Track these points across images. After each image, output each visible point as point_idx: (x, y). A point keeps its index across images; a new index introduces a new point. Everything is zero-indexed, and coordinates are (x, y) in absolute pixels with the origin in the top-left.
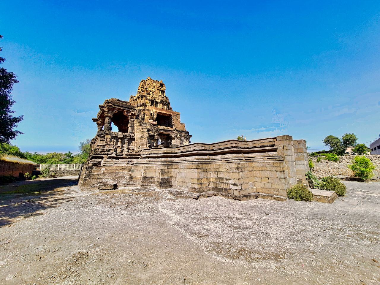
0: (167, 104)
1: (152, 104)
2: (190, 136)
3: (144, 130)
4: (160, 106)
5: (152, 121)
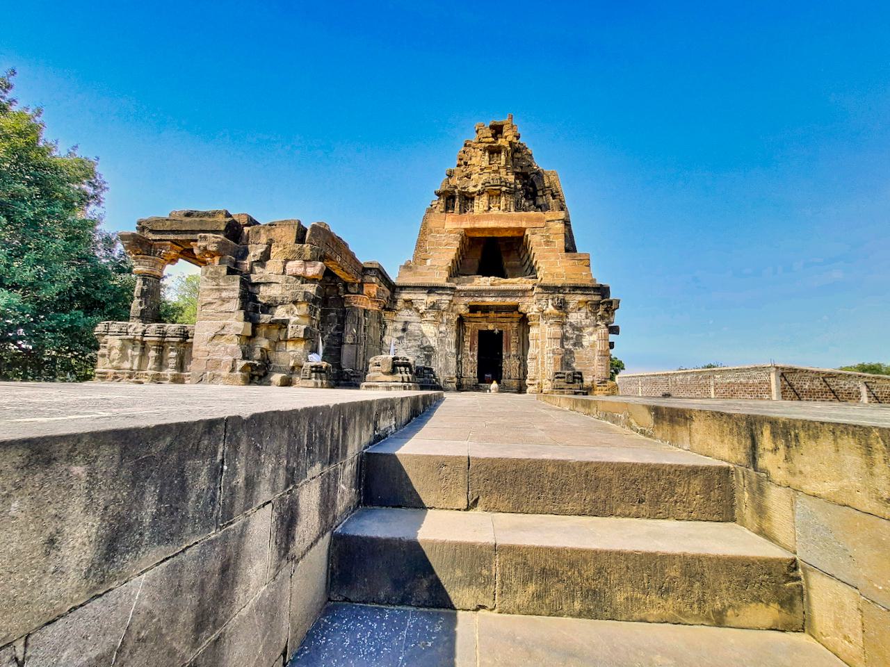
1: (448, 207)
2: (611, 302)
3: (227, 306)
4: (480, 204)
5: (298, 262)
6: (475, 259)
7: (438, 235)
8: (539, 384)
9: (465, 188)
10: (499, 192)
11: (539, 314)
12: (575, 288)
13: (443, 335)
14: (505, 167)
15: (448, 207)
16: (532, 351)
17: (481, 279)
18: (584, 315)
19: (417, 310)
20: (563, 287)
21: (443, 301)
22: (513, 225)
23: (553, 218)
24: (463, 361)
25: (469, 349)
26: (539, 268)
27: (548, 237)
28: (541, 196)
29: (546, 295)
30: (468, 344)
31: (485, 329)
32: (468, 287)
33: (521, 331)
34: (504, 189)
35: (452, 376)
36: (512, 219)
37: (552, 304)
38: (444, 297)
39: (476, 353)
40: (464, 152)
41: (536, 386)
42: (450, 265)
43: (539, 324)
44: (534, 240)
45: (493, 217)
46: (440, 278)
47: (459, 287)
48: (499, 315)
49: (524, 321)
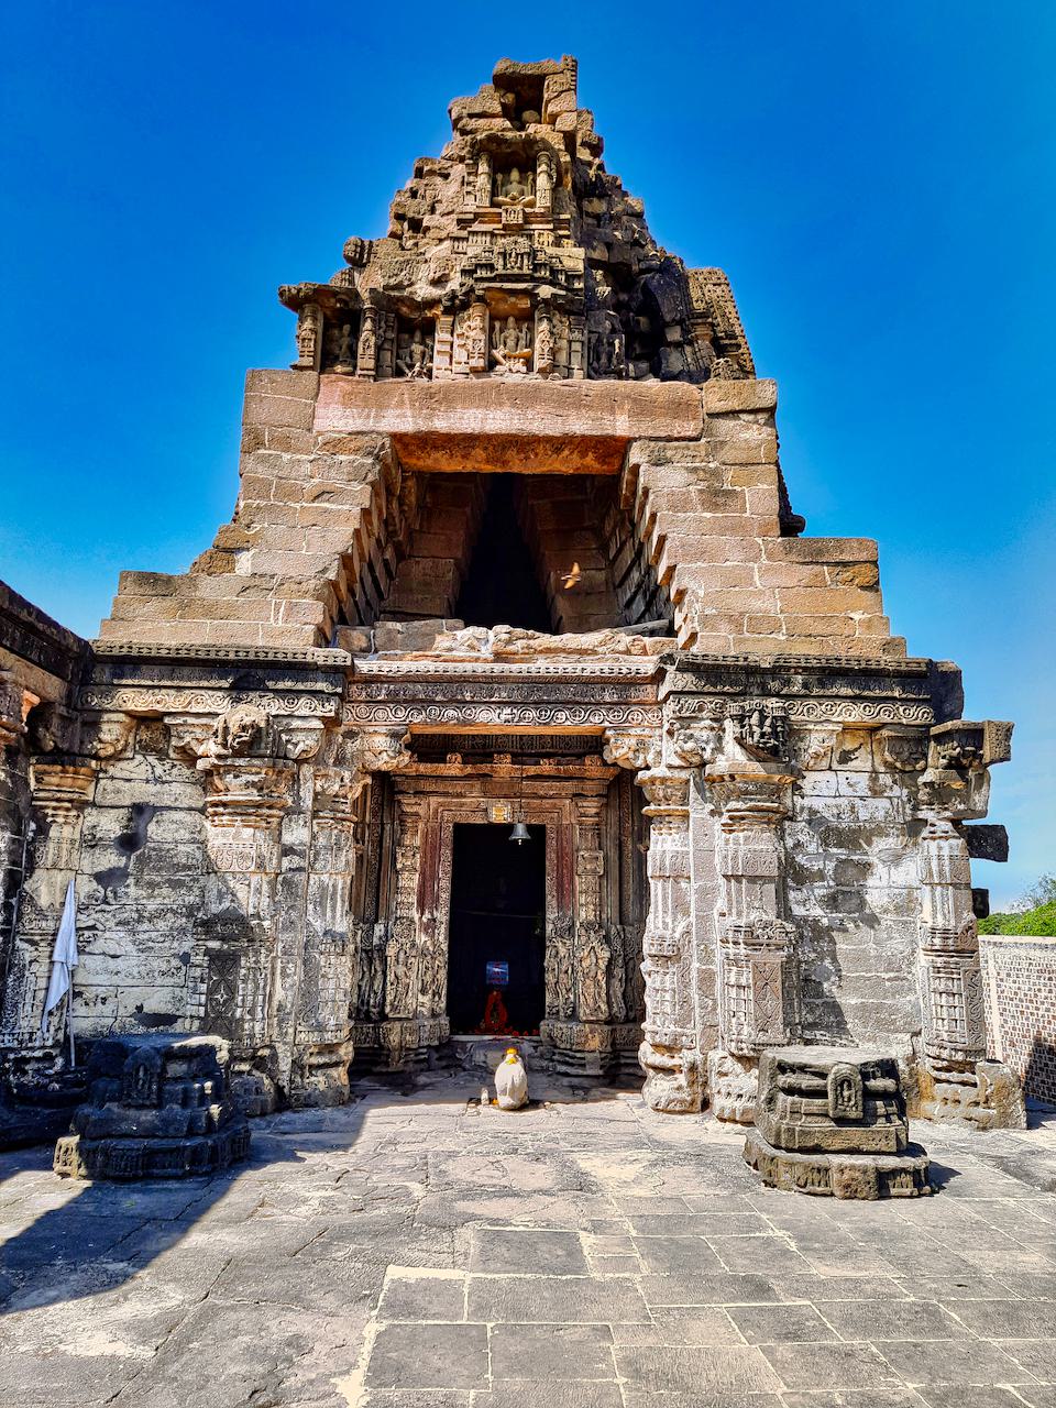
0: (551, 305)
2: (975, 734)
4: (457, 347)
6: (440, 561)
7: (286, 457)
8: (693, 1068)
9: (399, 287)
10: (525, 303)
11: (684, 775)
12: (828, 674)
13: (296, 861)
14: (552, 216)
15: (330, 356)
16: (660, 925)
17: (459, 634)
18: (863, 781)
19: (190, 758)
20: (780, 671)
21: (296, 723)
22: (580, 425)
23: (735, 405)
24: (391, 951)
25: (414, 899)
26: (681, 593)
27: (715, 474)
28: (678, 345)
29: (710, 703)
30: (410, 881)
31: (479, 820)
32: (407, 665)
33: (613, 830)
34: (545, 291)
35: (329, 1037)
36: (579, 402)
37: (740, 741)
38: (303, 706)
39: (442, 915)
40: (414, 194)
41: (682, 1079)
42: (331, 575)
43: (686, 816)
44: (664, 485)
45: (504, 398)
46: (288, 629)
47: (365, 666)
48: (532, 770)
49: (625, 793)
